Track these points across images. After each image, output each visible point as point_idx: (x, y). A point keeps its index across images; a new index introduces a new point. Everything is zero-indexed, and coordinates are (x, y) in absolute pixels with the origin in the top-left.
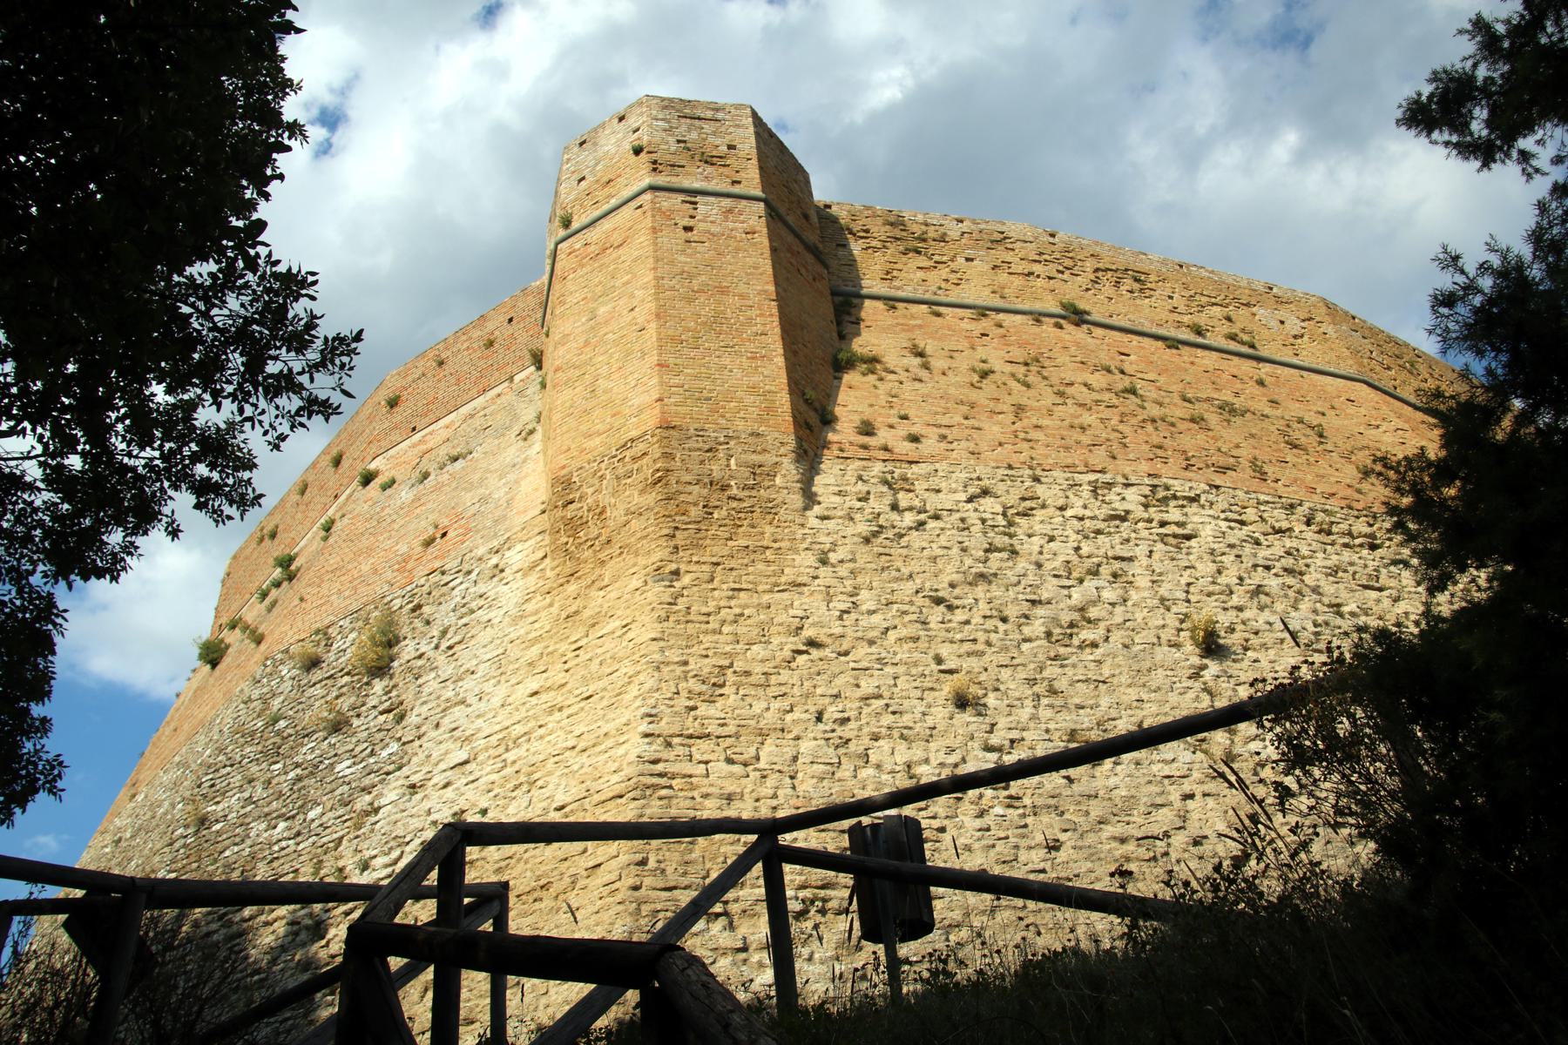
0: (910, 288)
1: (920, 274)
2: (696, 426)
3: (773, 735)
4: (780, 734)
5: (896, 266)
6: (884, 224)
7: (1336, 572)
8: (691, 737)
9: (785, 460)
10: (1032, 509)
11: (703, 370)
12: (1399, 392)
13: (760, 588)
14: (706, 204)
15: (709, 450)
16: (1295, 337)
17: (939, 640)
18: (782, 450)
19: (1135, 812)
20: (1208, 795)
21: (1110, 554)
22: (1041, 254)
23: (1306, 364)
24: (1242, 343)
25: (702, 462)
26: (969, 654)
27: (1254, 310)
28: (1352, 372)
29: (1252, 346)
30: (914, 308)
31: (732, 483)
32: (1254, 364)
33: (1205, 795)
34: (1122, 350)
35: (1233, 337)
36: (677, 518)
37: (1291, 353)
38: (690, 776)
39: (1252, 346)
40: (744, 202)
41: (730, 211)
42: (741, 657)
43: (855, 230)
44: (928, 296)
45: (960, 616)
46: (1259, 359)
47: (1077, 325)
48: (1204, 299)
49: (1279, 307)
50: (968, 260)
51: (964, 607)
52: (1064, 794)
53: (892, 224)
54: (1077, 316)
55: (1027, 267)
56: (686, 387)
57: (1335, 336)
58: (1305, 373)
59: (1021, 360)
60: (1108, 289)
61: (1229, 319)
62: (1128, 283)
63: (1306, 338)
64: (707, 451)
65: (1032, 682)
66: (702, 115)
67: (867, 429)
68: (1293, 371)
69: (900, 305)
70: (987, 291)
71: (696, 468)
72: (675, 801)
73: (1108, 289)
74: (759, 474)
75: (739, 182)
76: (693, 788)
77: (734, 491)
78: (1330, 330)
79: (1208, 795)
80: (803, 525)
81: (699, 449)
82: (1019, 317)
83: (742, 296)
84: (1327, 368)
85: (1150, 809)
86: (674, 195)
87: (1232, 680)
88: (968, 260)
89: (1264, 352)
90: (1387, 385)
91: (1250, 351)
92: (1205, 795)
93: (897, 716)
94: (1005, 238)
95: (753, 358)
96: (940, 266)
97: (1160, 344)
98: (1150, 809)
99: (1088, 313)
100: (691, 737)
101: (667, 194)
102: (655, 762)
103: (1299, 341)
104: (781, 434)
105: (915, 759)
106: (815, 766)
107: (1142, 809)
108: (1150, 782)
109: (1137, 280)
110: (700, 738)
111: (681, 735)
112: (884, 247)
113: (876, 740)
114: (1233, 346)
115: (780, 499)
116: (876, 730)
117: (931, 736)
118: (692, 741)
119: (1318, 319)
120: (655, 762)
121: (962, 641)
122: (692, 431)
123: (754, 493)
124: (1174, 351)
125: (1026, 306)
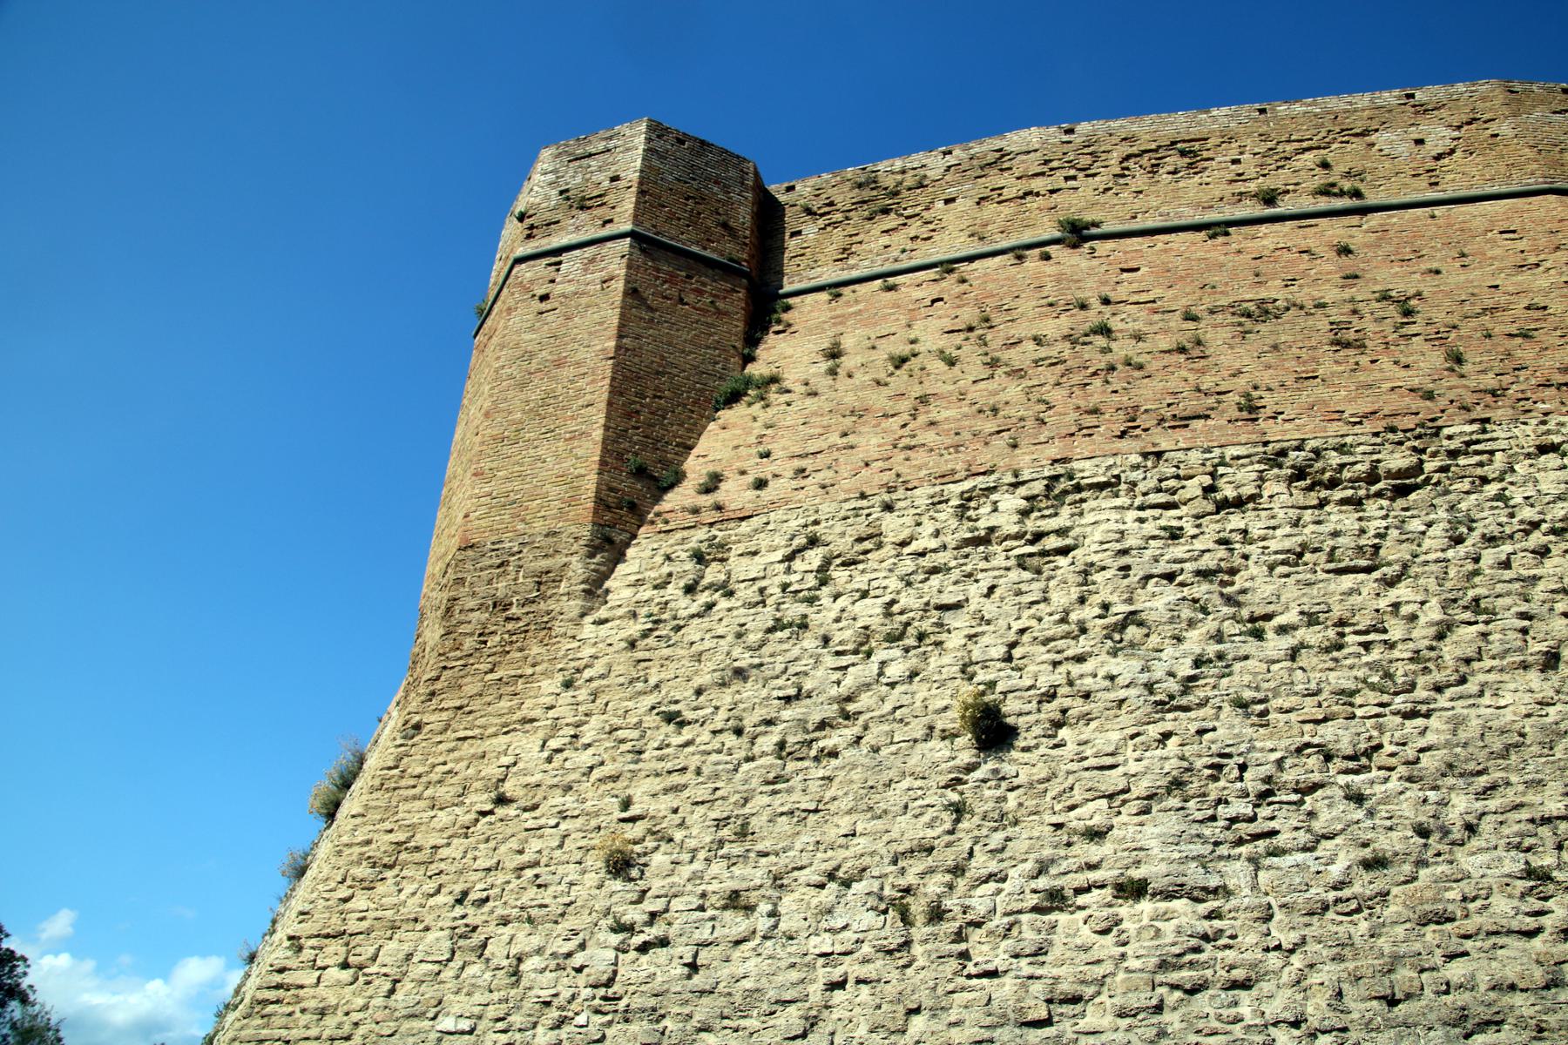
0: (866, 263)
1: (885, 240)
2: (494, 539)
3: (405, 927)
4: (410, 926)
5: (855, 239)
6: (853, 188)
7: (1300, 555)
8: (327, 936)
9: (574, 559)
10: (866, 552)
11: (517, 468)
13: (491, 730)
14: (570, 260)
15: (501, 565)
16: (1438, 157)
17: (644, 773)
18: (575, 547)
19: (755, 1013)
20: (865, 982)
21: (933, 602)
22: (1046, 162)
23: (1449, 194)
24: (1342, 194)
25: (490, 582)
26: (666, 791)
27: (1373, 138)
28: (1532, 183)
30: (862, 289)
31: (514, 600)
32: (1355, 220)
33: (859, 981)
34: (1125, 266)
35: (1326, 191)
36: (452, 654)
37: (1425, 184)
38: (302, 987)
39: (1357, 194)
40: (609, 244)
41: (592, 260)
42: (423, 828)
43: (815, 209)
44: (878, 270)
45: (687, 733)
47: (1075, 246)
48: (1289, 148)
49: (1419, 119)
50: (947, 201)
51: (697, 721)
52: (673, 990)
53: (860, 186)
54: (1077, 234)
55: (1024, 186)
56: (494, 494)
57: (1511, 133)
58: (1439, 211)
59: (964, 326)
60: (1140, 180)
61: (1325, 165)
62: (1174, 160)
63: (1458, 154)
64: (498, 567)
65: (720, 823)
66: (594, 151)
67: (712, 484)
68: (1419, 211)
69: (846, 291)
70: (963, 237)
71: (481, 589)
72: (273, 1019)
73: (1140, 180)
74: (544, 581)
75: (611, 221)
76: (298, 999)
77: (514, 610)
78: (1505, 128)
79: (865, 982)
80: (574, 637)
81: (491, 566)
82: (998, 259)
83: (578, 364)
84: (1489, 190)
85: (774, 1008)
86: (538, 261)
87: (1004, 784)
88: (947, 201)
89: (1372, 199)
91: (1355, 202)
92: (859, 981)
93: (543, 889)
94: (1003, 156)
95: (570, 439)
96: (909, 221)
97: (1202, 235)
98: (774, 1008)
99: (1096, 225)
100: (327, 936)
101: (532, 263)
102: (281, 971)
103: (1446, 161)
104: (580, 525)
105: (527, 949)
106: (423, 964)
107: (765, 1007)
108: (793, 965)
109: (1183, 153)
110: (334, 937)
111: (318, 936)
112: (847, 218)
113: (505, 925)
114: (1324, 203)
115: (558, 609)
116: (506, 912)
117: (563, 915)
118: (326, 941)
119: (1486, 116)
120: (281, 971)
121: (669, 772)
122: (489, 546)
123: (533, 608)
124: (1221, 239)
125: (1005, 244)
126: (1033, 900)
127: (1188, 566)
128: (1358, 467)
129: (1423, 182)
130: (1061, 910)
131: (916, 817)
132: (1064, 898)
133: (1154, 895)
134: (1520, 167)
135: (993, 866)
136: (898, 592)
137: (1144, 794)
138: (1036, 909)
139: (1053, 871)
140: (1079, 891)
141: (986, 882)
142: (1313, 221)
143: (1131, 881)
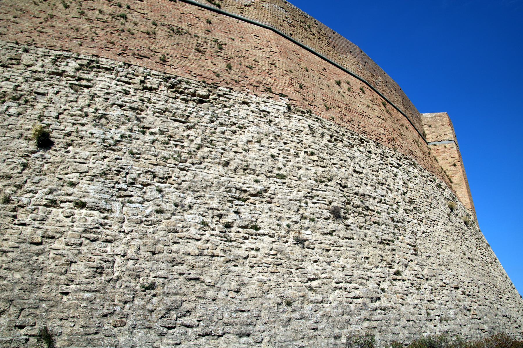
7: (164, 112)
10: (13, 64)
12: (294, 38)
16: (246, 6)
21: (35, 90)
24: (215, 4)
28: (268, 25)
29: (219, 6)
32: (216, 14)
37: (239, 12)
39: (219, 6)
46: (219, 12)
57: (267, 8)
58: (240, 22)
63: (251, 7)
68: (235, 19)
87: (44, 161)
89: (223, 10)
90: (287, 33)
91: (217, 8)
103: (247, 8)
126: (45, 202)
127: (128, 105)
128: (191, 90)
129: (239, 11)
130: (54, 207)
131: (8, 165)
132: (56, 203)
133: (87, 208)
134: (267, 19)
135: (33, 188)
136: (22, 83)
137: (93, 174)
138: (45, 205)
139: (55, 193)
140: (62, 202)
141: (29, 193)
142: (203, 9)
143: (81, 202)
